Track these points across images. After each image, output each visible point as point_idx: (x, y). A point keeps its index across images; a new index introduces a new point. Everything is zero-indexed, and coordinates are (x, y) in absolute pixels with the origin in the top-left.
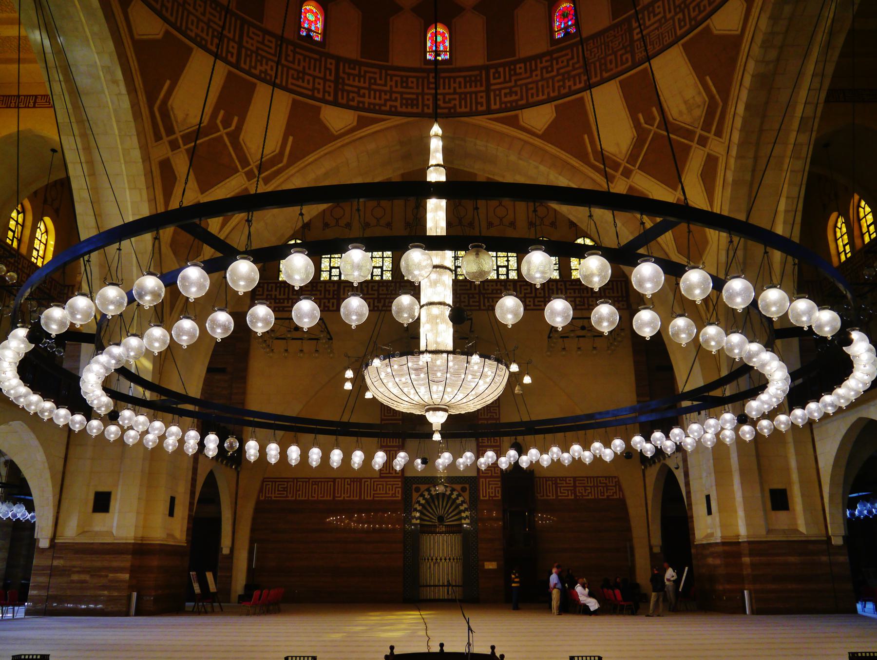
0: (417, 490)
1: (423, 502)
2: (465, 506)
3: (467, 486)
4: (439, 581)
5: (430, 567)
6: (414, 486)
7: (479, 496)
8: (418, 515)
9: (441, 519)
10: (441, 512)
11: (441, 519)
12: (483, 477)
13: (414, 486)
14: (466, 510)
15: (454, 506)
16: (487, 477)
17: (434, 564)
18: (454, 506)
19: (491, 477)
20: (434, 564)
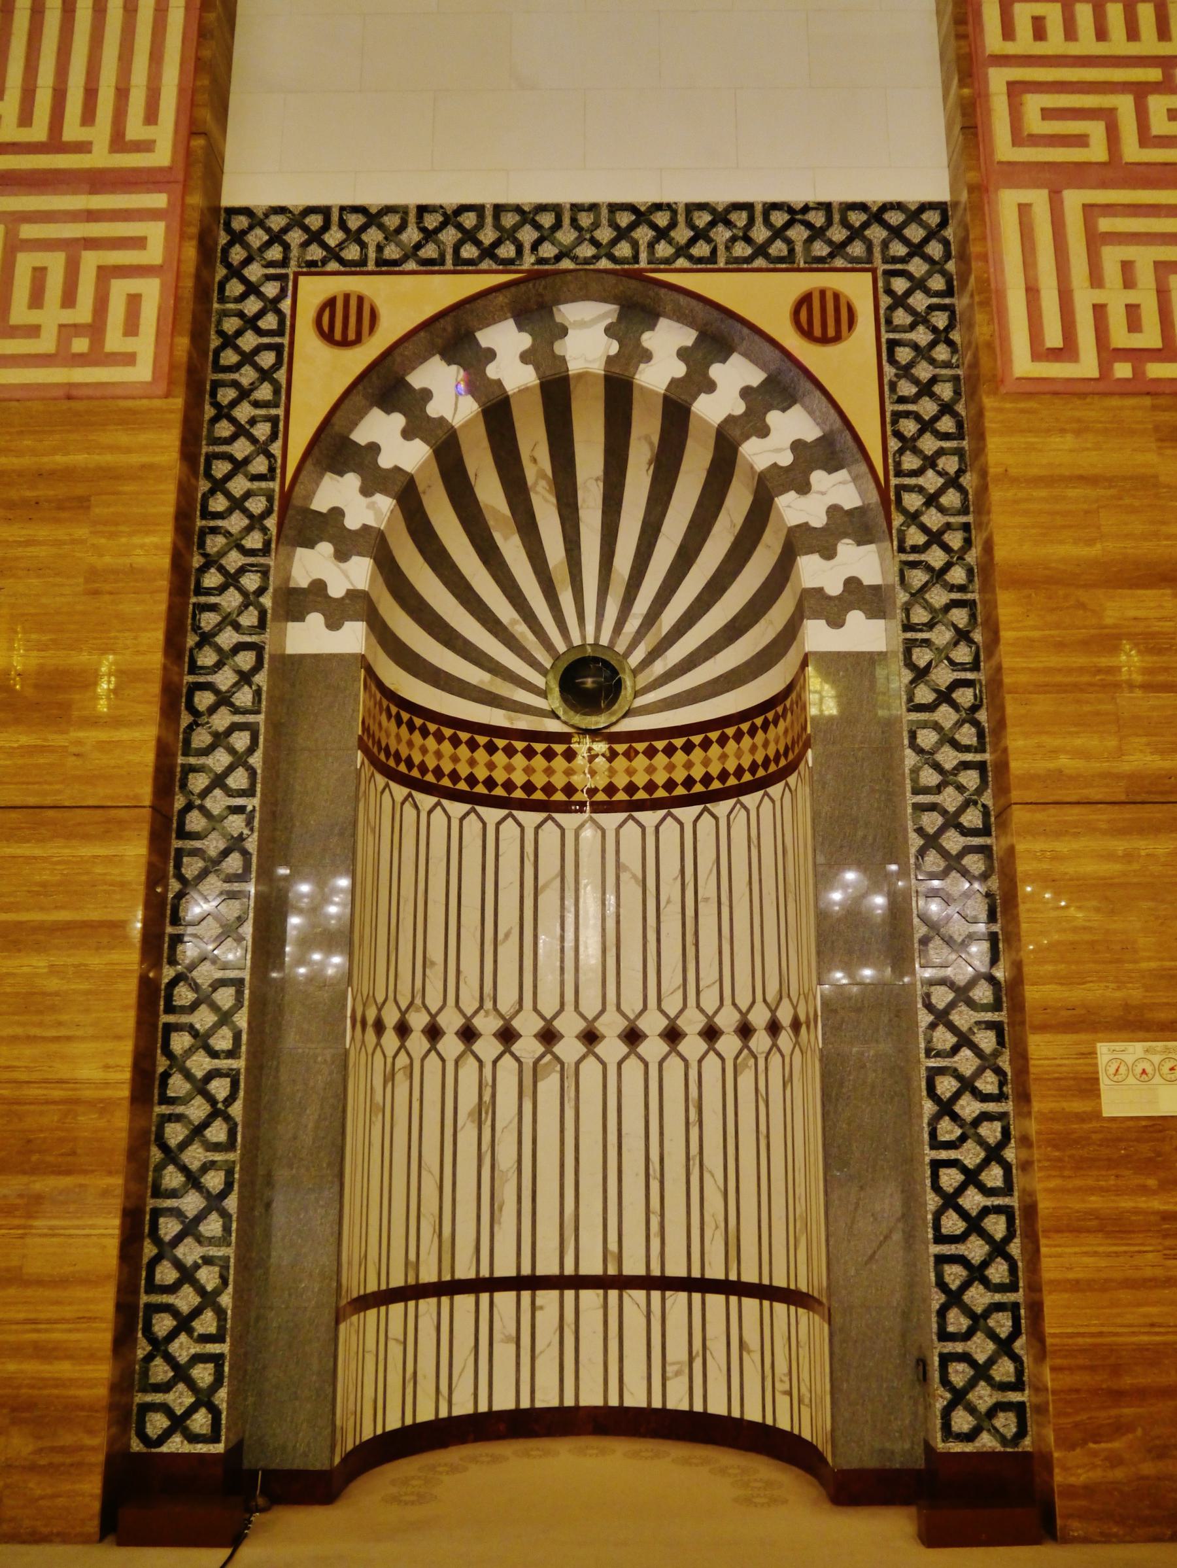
0: (342, 324)
1: (407, 455)
2: (837, 490)
3: (857, 288)
4: (569, 1231)
5: (485, 1110)
6: (314, 291)
7: (1000, 345)
8: (359, 572)
9: (590, 681)
10: (591, 627)
11: (590, 681)
12: (1018, 174)
13: (314, 291)
14: (848, 525)
15: (737, 503)
16: (1080, 175)
17: (528, 1088)
18: (737, 503)
19: (1115, 172)
20: (528, 1088)
